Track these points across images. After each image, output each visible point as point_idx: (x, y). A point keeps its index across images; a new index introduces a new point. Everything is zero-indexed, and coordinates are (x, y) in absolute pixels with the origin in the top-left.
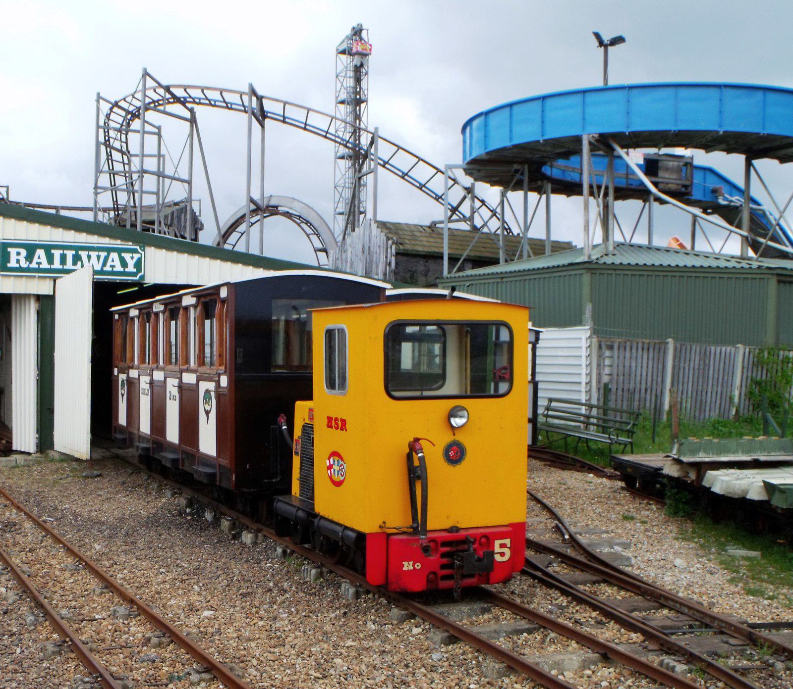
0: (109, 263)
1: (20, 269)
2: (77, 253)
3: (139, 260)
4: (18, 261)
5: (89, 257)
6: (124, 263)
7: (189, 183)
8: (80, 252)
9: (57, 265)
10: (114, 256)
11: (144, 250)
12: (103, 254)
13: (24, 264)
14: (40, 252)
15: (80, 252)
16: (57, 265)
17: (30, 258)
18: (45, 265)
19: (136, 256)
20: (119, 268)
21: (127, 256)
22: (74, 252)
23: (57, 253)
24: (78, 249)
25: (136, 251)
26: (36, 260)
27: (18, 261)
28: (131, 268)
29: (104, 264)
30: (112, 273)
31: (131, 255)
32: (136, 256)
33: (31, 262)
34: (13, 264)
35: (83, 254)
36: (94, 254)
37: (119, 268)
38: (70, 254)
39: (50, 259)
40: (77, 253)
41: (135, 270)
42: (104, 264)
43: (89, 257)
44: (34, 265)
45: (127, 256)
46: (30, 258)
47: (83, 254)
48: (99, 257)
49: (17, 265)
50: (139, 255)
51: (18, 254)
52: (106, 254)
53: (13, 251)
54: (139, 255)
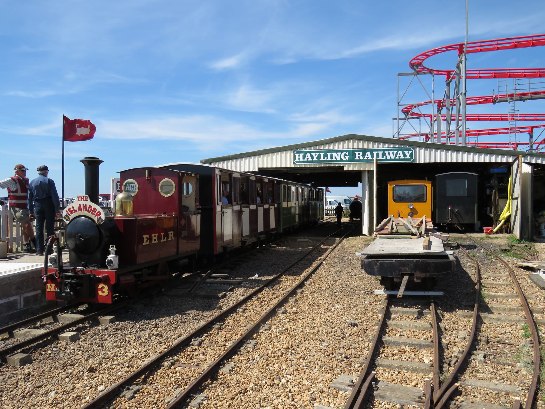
0: (398, 155)
1: (360, 160)
2: (384, 152)
3: (412, 153)
4: (359, 157)
5: (389, 154)
8: (385, 152)
11: (414, 149)
12: (395, 152)
13: (361, 158)
14: (368, 153)
15: (385, 152)
17: (364, 155)
19: (410, 152)
20: (402, 157)
21: (406, 152)
22: (382, 152)
23: (375, 153)
24: (384, 150)
25: (410, 150)
26: (366, 156)
27: (359, 157)
28: (408, 157)
29: (396, 156)
31: (408, 151)
32: (410, 152)
33: (364, 157)
34: (357, 158)
35: (387, 153)
36: (391, 152)
37: (402, 157)
38: (381, 153)
40: (384, 152)
41: (410, 158)
42: (396, 156)
43: (389, 154)
44: (366, 158)
45: (406, 152)
46: (364, 155)
47: (387, 153)
48: (393, 153)
49: (359, 159)
50: (412, 151)
51: (359, 154)
52: (396, 152)
53: (357, 153)
54: (412, 151)
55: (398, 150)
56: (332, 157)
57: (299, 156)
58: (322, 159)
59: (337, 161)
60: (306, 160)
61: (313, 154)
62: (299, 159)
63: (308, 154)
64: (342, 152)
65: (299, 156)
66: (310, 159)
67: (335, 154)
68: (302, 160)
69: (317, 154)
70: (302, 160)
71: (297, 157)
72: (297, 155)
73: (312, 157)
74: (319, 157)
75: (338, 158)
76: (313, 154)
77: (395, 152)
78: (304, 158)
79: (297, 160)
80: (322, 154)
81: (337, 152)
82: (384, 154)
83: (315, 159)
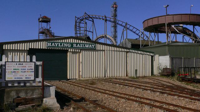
1: (75, 47)
6: (92, 46)
7: (93, 32)
9: (81, 47)
10: (90, 45)
12: (89, 45)
14: (78, 45)
16: (81, 47)
17: (77, 46)
18: (79, 47)
23: (81, 45)
24: (84, 44)
28: (93, 47)
30: (90, 48)
34: (74, 46)
35: (85, 45)
36: (87, 45)
38: (83, 45)
39: (80, 46)
46: (77, 46)
47: (85, 45)
53: (74, 44)
55: (90, 44)
56: (64, 45)
57: (49, 44)
58: (59, 46)
59: (66, 47)
60: (52, 46)
61: (56, 44)
62: (49, 45)
63: (53, 43)
64: (68, 43)
65: (49, 44)
66: (54, 46)
67: (65, 44)
68: (50, 46)
69: (57, 44)
70: (50, 46)
71: (48, 44)
72: (48, 43)
73: (55, 45)
74: (58, 45)
75: (66, 46)
76: (56, 44)
77: (89, 45)
78: (51, 45)
79: (48, 45)
80: (59, 44)
81: (66, 43)
82: (84, 46)
83: (56, 46)
